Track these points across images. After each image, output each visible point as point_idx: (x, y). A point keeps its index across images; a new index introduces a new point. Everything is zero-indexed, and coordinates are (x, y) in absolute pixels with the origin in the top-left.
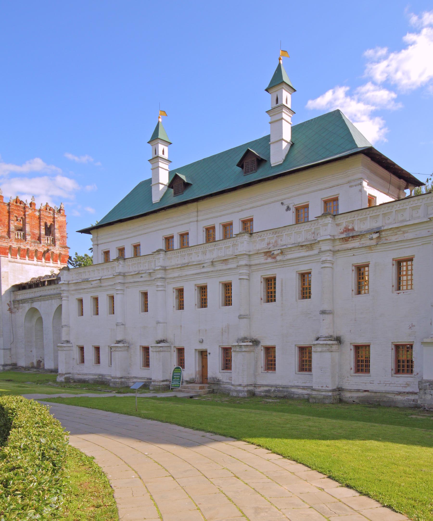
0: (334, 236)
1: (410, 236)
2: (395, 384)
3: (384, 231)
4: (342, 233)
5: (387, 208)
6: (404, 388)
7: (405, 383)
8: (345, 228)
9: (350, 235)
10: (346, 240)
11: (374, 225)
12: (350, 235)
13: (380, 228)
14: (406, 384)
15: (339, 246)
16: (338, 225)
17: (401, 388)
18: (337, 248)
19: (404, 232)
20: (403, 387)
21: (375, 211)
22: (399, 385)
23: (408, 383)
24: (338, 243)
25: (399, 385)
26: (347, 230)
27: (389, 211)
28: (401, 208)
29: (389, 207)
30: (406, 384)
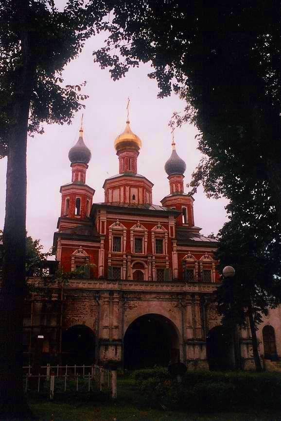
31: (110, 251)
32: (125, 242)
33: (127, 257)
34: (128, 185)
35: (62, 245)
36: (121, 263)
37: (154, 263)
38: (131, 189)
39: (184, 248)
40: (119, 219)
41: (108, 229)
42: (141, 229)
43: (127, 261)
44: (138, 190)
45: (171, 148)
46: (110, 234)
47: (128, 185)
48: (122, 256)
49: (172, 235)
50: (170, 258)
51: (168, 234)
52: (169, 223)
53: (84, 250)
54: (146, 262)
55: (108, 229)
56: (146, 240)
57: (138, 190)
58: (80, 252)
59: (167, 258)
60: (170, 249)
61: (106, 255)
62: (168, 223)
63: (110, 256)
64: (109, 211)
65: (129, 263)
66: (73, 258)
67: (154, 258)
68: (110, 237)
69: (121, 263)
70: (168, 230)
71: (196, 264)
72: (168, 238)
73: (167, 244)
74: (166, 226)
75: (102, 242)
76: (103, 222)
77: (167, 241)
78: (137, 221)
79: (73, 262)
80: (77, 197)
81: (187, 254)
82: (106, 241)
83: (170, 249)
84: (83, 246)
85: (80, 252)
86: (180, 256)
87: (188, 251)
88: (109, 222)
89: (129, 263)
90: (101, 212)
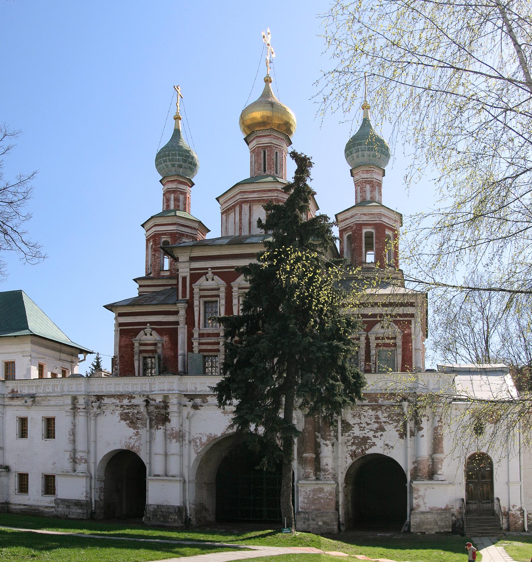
0: (4, 395)
1: (52, 403)
3: (38, 396)
4: (10, 393)
8: (12, 390)
9: (14, 396)
10: (12, 398)
11: (33, 391)
12: (14, 396)
13: (34, 394)
15: (7, 402)
16: (7, 387)
18: (6, 403)
19: (49, 400)
24: (6, 400)
26: (13, 391)
34: (246, 202)
36: (215, 347)
40: (212, 268)
41: (192, 290)
46: (196, 297)
48: (218, 335)
53: (153, 329)
61: (190, 335)
63: (196, 336)
66: (136, 345)
68: (196, 303)
69: (215, 347)
75: (182, 312)
79: (136, 350)
84: (152, 323)
88: (195, 276)
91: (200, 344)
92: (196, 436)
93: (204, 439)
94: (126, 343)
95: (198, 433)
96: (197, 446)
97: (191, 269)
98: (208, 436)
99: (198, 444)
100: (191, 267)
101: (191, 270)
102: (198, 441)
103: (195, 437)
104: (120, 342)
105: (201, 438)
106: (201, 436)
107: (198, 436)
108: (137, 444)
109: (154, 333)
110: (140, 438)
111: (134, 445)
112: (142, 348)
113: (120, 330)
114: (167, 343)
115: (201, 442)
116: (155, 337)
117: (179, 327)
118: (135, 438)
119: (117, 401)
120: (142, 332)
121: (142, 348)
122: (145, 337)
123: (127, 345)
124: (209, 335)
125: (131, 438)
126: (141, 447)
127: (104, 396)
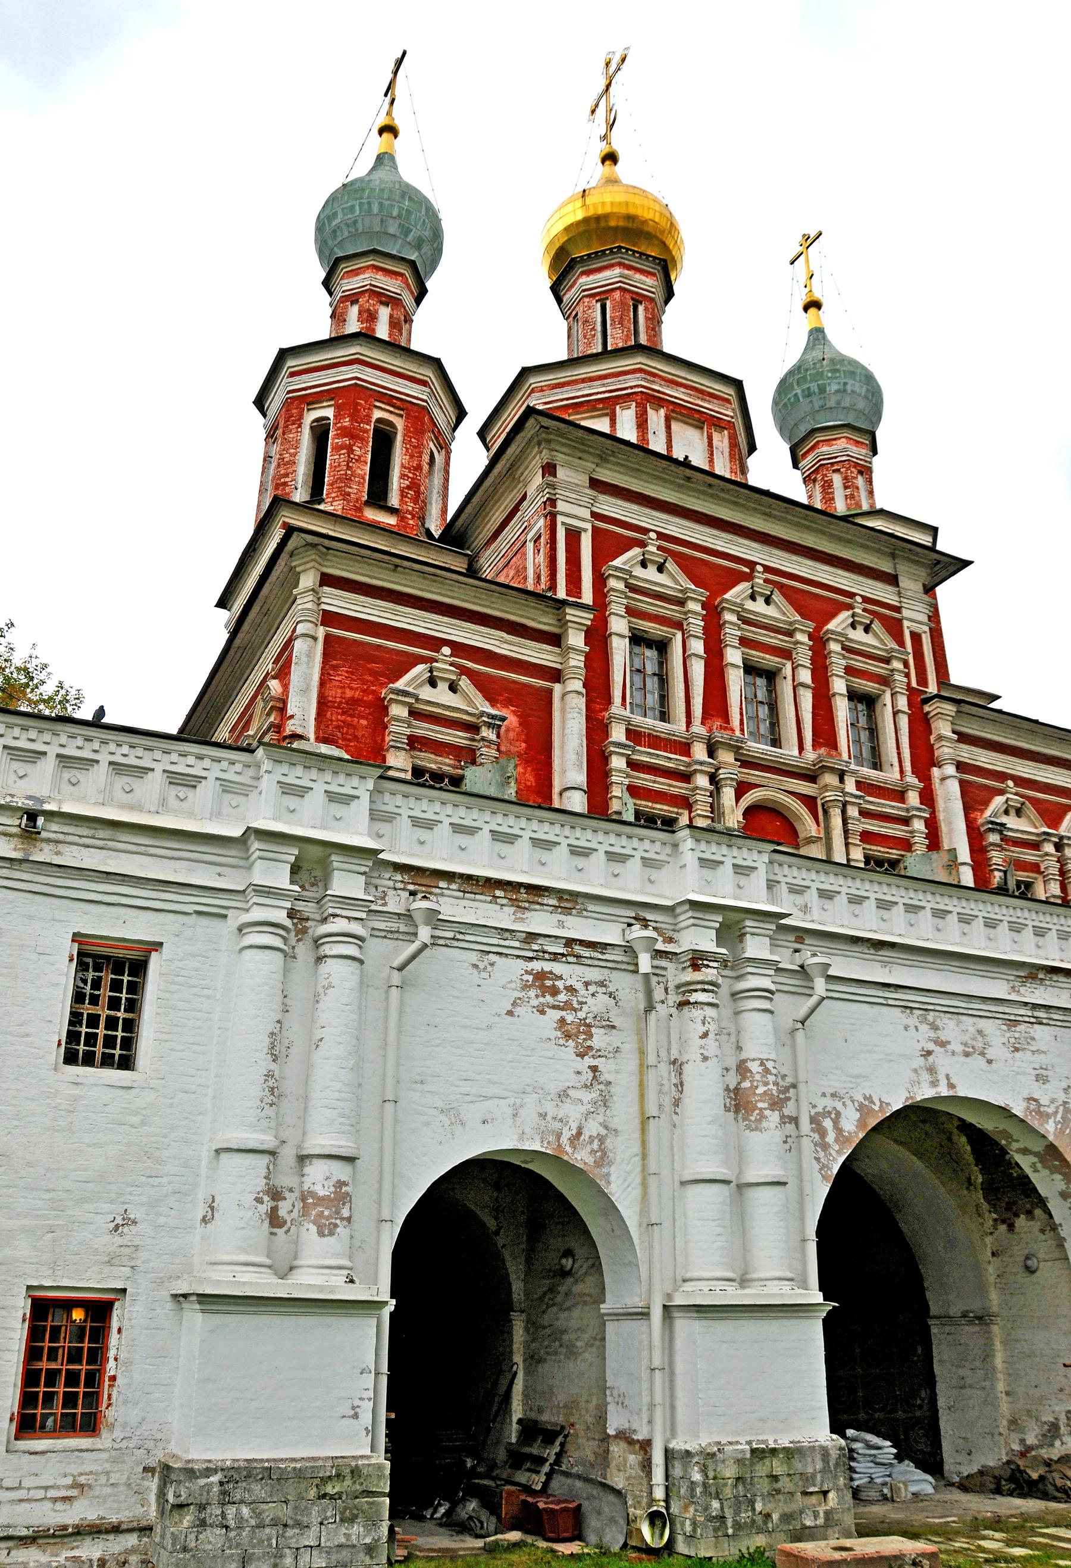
2: (19, 1487)
5: (80, 742)
6: (59, 1506)
7: (69, 1481)
14: (75, 1485)
17: (48, 1505)
20: (55, 1500)
21: (32, 734)
22: (40, 1494)
23: (82, 1480)
25: (40, 1494)
27: (86, 754)
28: (131, 761)
29: (88, 740)
30: (75, 1485)
31: (616, 708)
32: (698, 670)
33: (711, 754)
34: (659, 402)
35: (329, 618)
36: (677, 788)
37: (853, 812)
38: (674, 426)
39: (985, 759)
42: (771, 611)
43: (713, 778)
44: (710, 439)
45: (805, 322)
47: (659, 402)
49: (922, 680)
50: (928, 797)
51: (906, 664)
52: (905, 613)
53: (464, 671)
54: (809, 802)
55: (600, 581)
56: (805, 676)
57: (710, 439)
58: (443, 686)
59: (913, 798)
60: (924, 760)
61: (597, 729)
62: (898, 609)
63: (618, 733)
64: (606, 475)
65: (728, 794)
66: (398, 711)
67: (850, 786)
69: (677, 788)
70: (901, 643)
71: (1049, 848)
72: (909, 688)
73: (904, 722)
74: (894, 628)
75: (576, 639)
76: (573, 536)
77: (903, 703)
78: (751, 565)
80: (377, 414)
81: (1002, 792)
82: (598, 637)
83: (924, 760)
84: (459, 649)
85: (443, 686)
86: (973, 800)
87: (1002, 776)
88: (610, 543)
89: (728, 794)
90: (561, 473)
91: (632, 764)
92: (822, 1103)
93: (850, 1122)
94: (349, 693)
95: (829, 1091)
96: (825, 1147)
97: (594, 515)
98: (864, 1110)
99: (831, 1138)
100: (595, 509)
101: (594, 515)
102: (828, 1123)
103: (820, 1109)
104: (322, 684)
105: (838, 1114)
106: (839, 1106)
107: (829, 1103)
108: (592, 1128)
109: (464, 683)
110: (605, 1101)
111: (579, 1133)
112: (424, 729)
113: (328, 637)
114: (511, 735)
115: (839, 1130)
116: (470, 702)
117: (557, 688)
118: (587, 1096)
119: (498, 914)
120: (420, 667)
121: (424, 729)
122: (428, 688)
123: (353, 702)
124: (656, 741)
125: (563, 1095)
126: (608, 1143)
127: (449, 876)
